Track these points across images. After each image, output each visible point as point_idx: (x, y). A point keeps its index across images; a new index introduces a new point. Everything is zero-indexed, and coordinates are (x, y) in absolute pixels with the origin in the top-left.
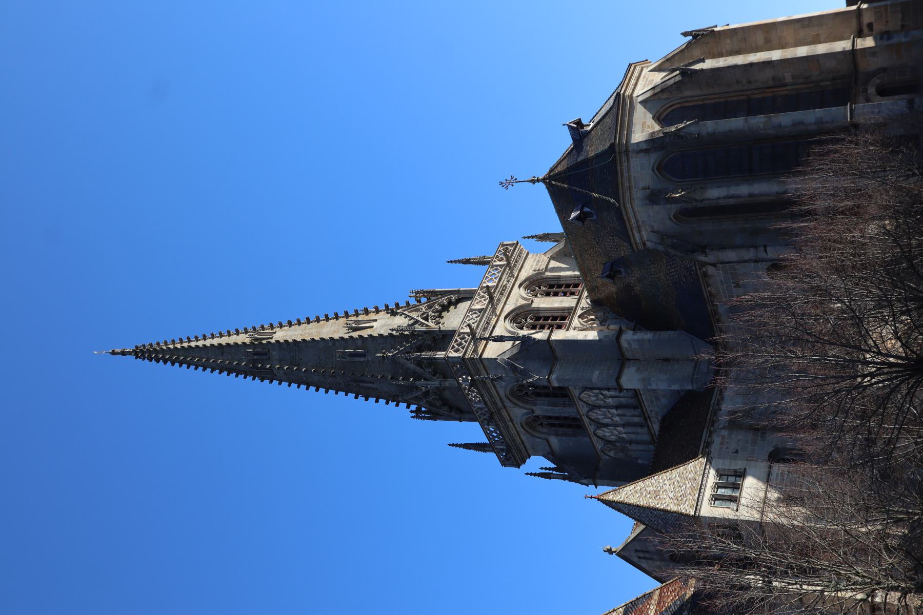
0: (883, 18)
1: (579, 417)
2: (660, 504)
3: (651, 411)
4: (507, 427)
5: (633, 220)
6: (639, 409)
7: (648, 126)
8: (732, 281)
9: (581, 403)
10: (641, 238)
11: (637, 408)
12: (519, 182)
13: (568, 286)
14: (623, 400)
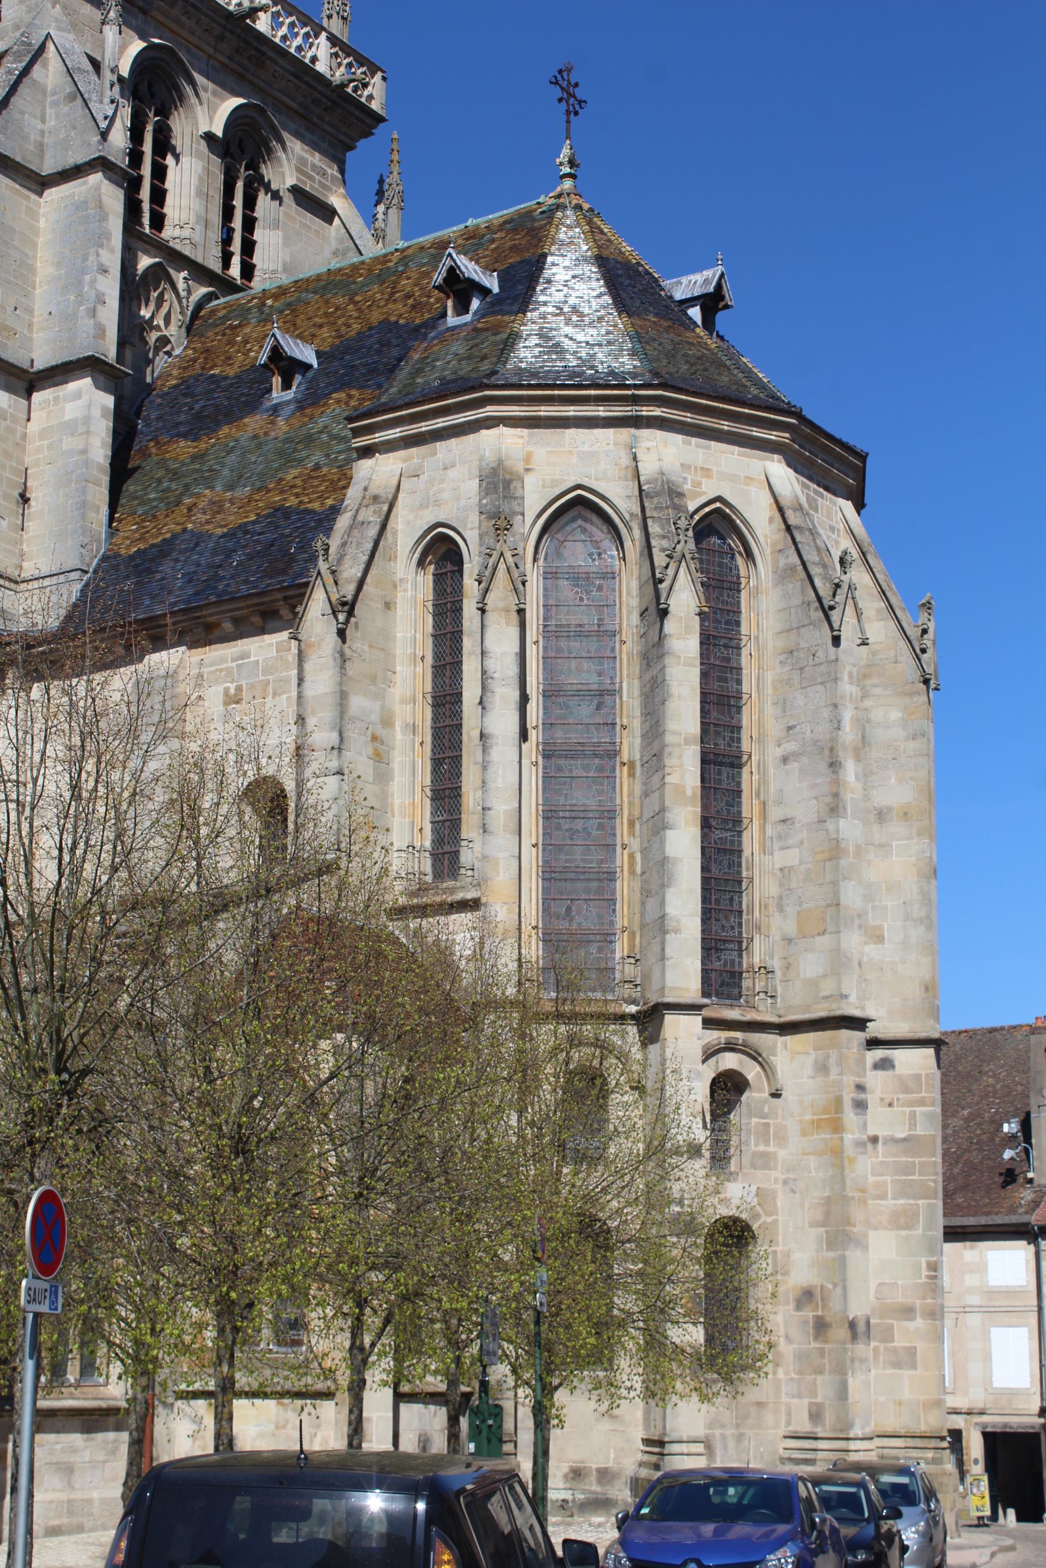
0: (901, 1096)
5: (440, 423)
7: (699, 484)
8: (244, 683)
10: (389, 447)
12: (568, 122)
13: (248, 247)
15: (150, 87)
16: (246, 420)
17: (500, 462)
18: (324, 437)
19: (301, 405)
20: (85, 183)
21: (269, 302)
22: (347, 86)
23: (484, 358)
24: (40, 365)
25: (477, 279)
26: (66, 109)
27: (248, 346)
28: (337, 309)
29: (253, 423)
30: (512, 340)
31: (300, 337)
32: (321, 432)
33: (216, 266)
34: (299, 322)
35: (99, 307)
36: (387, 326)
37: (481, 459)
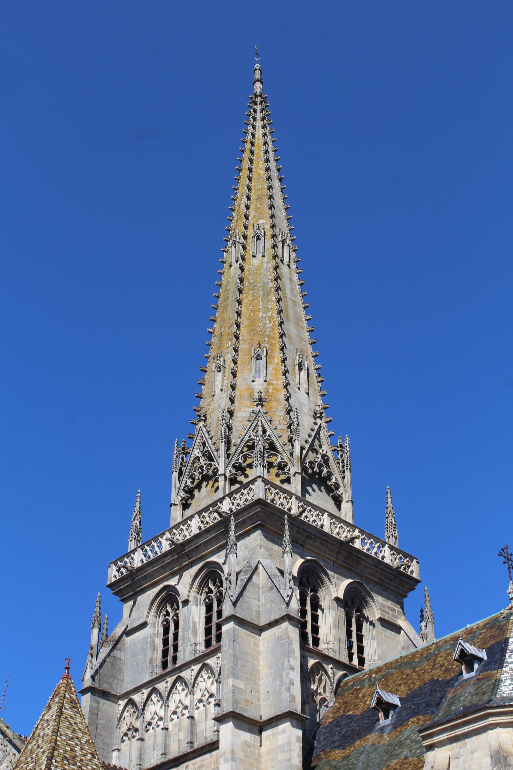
1: (179, 663)
2: (56, 764)
3: (187, 767)
4: (164, 568)
6: (190, 749)
9: (199, 666)
11: (191, 747)
12: (510, 572)
13: (361, 650)
14: (200, 728)
15: (307, 579)
16: (368, 736)
17: (500, 747)
18: (408, 741)
19: (395, 726)
20: (280, 628)
21: (373, 676)
22: (400, 568)
23: (484, 694)
24: (264, 718)
25: (475, 654)
26: (269, 594)
27: (365, 699)
28: (407, 675)
29: (372, 737)
30: (497, 683)
31: (390, 691)
32: (406, 739)
33: (346, 660)
34: (389, 684)
35: (291, 686)
36: (433, 682)
37: (490, 746)
